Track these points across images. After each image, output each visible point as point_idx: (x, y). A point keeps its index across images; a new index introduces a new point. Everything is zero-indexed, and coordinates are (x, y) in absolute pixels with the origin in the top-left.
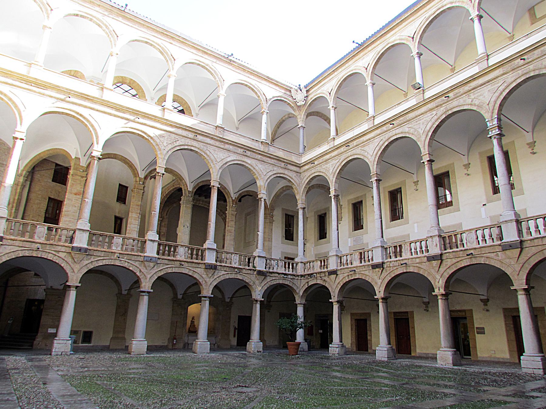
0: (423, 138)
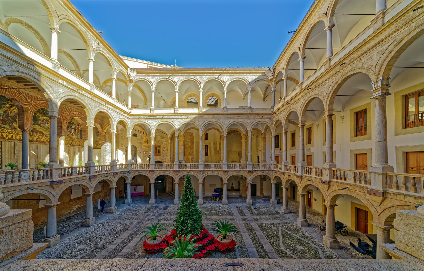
0: (326, 99)
